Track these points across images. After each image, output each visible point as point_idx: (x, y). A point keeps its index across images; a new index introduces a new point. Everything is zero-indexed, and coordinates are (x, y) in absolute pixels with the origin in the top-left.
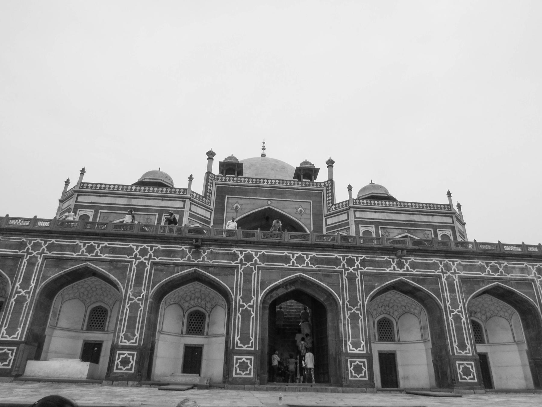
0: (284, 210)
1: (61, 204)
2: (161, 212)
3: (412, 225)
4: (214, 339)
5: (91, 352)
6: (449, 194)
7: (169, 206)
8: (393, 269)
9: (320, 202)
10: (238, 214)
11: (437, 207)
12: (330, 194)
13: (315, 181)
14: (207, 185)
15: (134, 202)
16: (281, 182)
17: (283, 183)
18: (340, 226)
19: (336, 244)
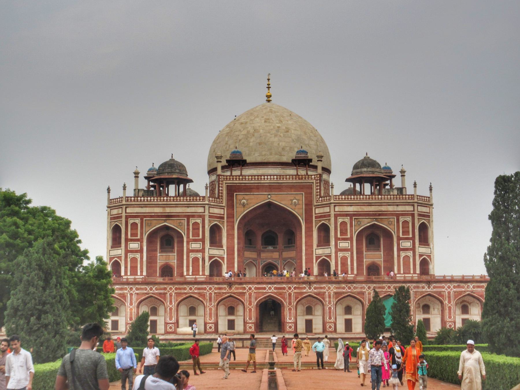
0: (282, 202)
1: (109, 209)
2: (189, 217)
3: (380, 215)
4: (239, 317)
5: (192, 323)
6: (415, 185)
7: (193, 211)
8: (307, 290)
9: (311, 193)
10: (245, 209)
11: (403, 198)
12: (318, 187)
13: (311, 164)
14: (219, 187)
15: (168, 210)
16: (278, 177)
17: (280, 178)
18: (325, 216)
19: (284, 281)
